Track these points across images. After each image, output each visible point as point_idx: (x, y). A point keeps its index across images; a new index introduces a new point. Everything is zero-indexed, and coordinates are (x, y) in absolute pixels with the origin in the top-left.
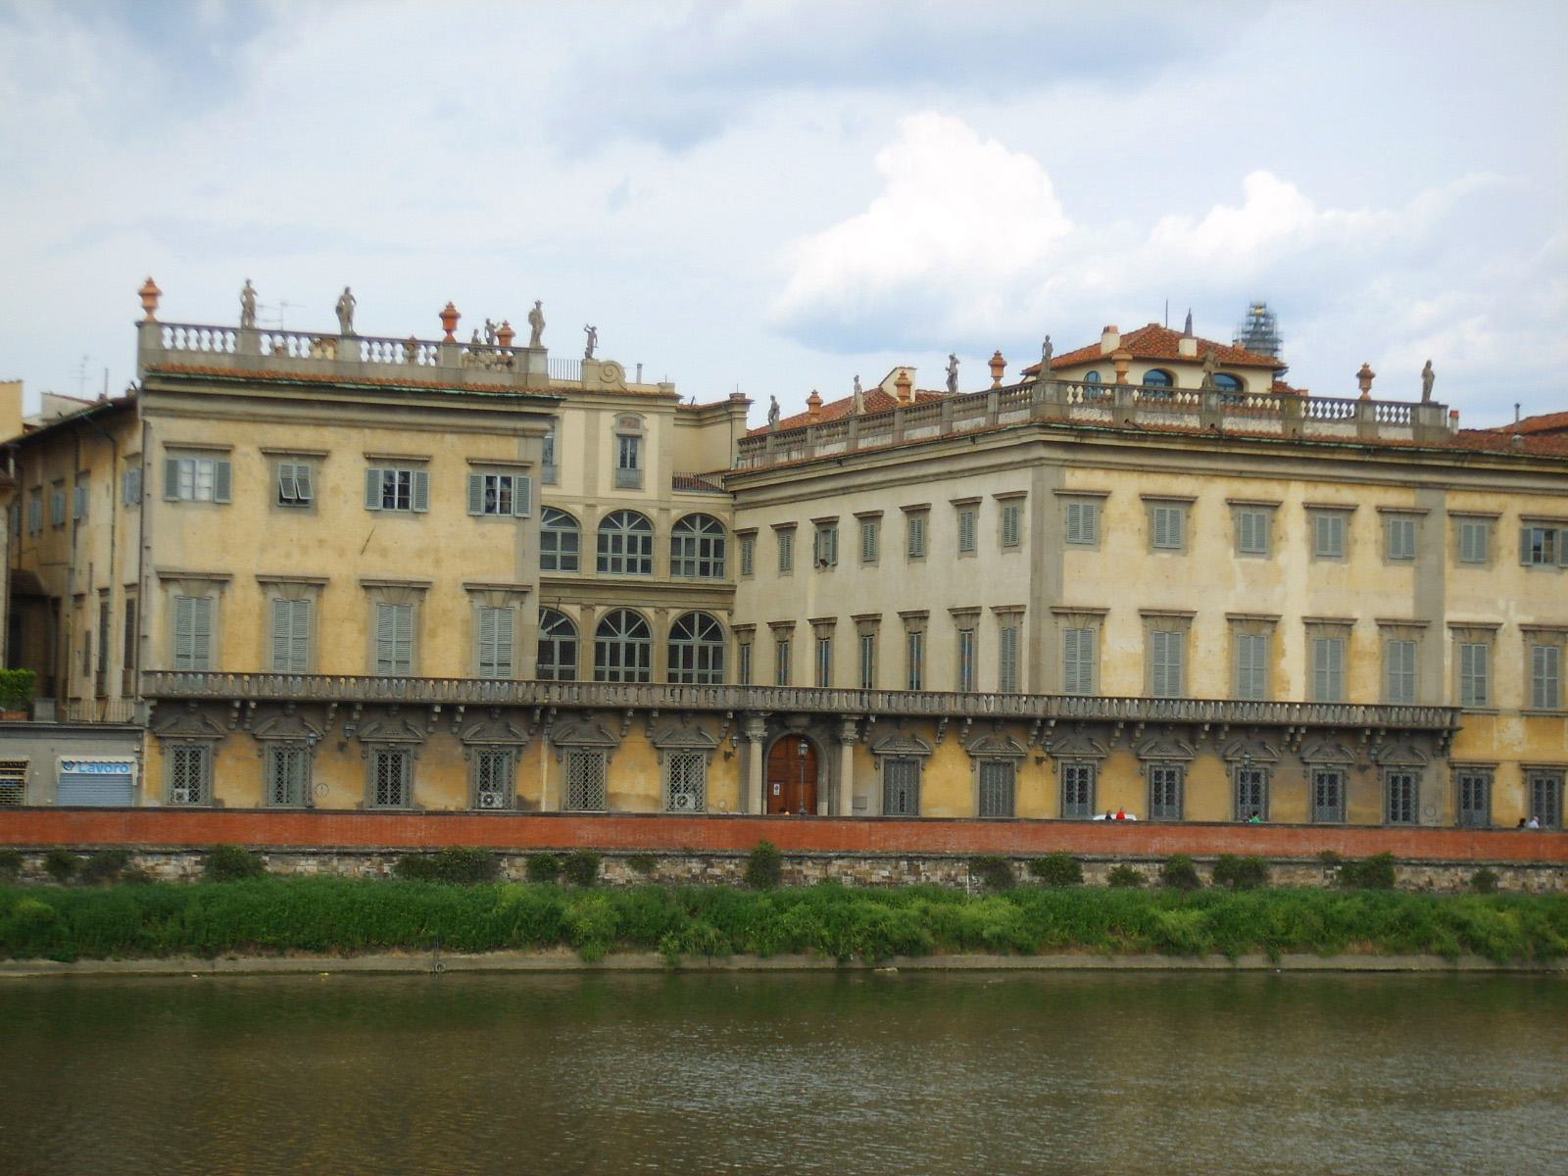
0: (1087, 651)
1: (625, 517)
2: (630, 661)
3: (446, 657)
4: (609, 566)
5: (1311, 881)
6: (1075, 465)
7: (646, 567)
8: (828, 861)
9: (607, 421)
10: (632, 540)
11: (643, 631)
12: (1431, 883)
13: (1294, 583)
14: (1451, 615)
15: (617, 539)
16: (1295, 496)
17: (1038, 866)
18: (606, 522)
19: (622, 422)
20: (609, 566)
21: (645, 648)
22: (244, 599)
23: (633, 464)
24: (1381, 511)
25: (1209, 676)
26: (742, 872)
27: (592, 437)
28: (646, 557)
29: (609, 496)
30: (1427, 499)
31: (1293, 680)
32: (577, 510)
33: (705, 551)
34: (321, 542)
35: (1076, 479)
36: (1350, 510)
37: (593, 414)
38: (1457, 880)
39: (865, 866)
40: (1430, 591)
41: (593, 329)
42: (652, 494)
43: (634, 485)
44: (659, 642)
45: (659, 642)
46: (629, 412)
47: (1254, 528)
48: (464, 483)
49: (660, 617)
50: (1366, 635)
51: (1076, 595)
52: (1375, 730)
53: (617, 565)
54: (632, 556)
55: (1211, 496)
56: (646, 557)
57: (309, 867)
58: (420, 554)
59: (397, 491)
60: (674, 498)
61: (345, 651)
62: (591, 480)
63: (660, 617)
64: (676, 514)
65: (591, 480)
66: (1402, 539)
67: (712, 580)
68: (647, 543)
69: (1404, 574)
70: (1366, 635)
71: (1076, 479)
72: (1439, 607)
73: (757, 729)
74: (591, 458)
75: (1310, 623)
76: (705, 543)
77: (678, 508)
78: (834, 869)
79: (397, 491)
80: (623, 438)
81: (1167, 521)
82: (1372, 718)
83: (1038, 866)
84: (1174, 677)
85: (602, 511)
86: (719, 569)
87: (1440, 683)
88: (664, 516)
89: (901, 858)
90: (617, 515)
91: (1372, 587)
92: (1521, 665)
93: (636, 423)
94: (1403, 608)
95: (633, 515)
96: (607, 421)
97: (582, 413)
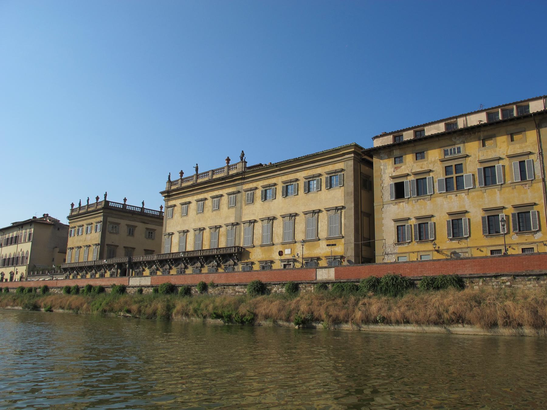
13: (210, 219)
30: (239, 188)
40: (239, 215)
69: (233, 210)
91: (226, 215)
94: (232, 220)
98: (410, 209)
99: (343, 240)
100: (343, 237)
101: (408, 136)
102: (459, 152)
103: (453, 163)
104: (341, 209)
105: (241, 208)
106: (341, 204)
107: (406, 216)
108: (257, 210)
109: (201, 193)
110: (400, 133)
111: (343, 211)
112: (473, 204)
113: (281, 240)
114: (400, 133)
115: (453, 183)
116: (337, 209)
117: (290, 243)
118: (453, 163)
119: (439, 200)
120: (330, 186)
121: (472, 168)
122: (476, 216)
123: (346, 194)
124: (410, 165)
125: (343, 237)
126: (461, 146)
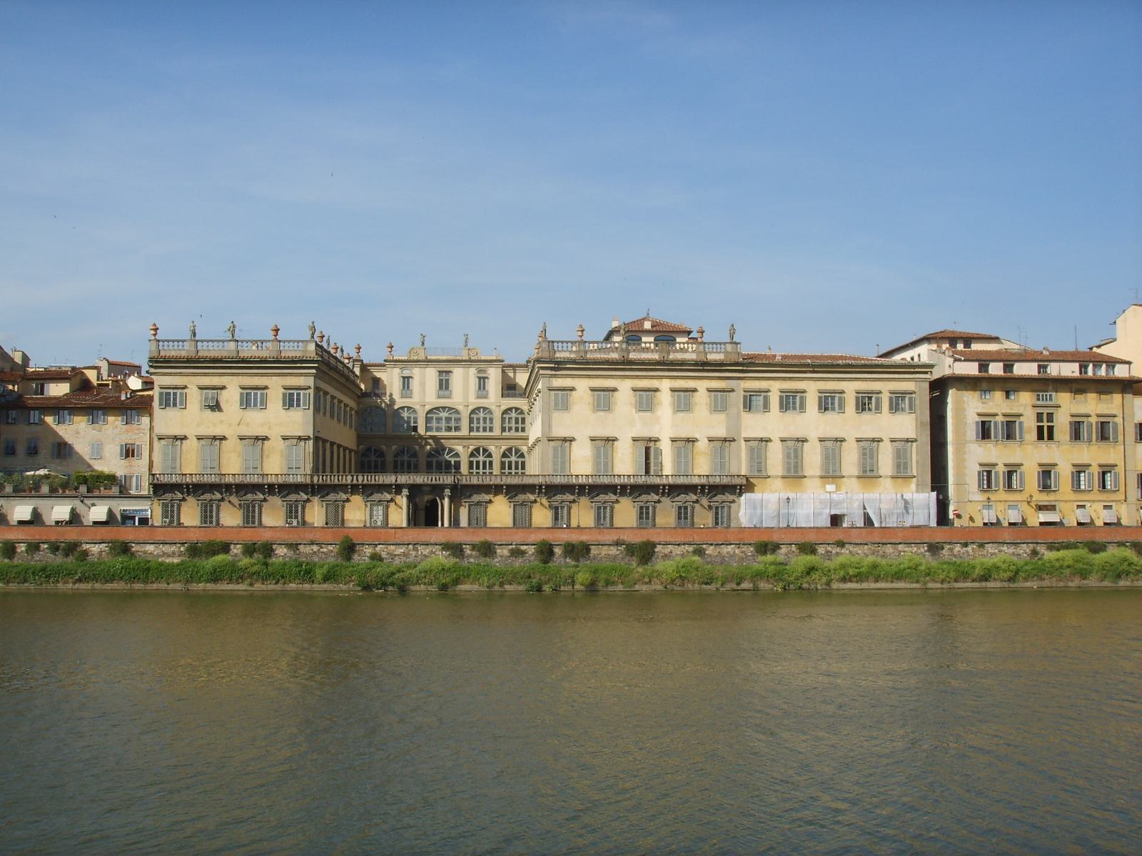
0: (563, 455)
2: (484, 468)
3: (275, 466)
4: (475, 430)
5: (610, 552)
6: (555, 376)
7: (491, 429)
8: (376, 545)
9: (472, 371)
11: (490, 455)
12: (671, 552)
13: (665, 423)
14: (745, 435)
16: (665, 385)
17: (474, 547)
18: (473, 412)
20: (475, 430)
21: (491, 463)
22: (191, 446)
23: (447, 388)
24: (673, 390)
25: (625, 465)
26: (335, 550)
27: (466, 378)
28: (523, 426)
29: (474, 402)
31: (668, 468)
32: (460, 408)
33: (517, 422)
34: (222, 422)
35: (558, 383)
36: (695, 390)
37: (466, 369)
38: (685, 551)
39: (392, 547)
40: (736, 424)
43: (486, 397)
44: (496, 460)
45: (496, 460)
47: (646, 399)
48: (281, 396)
49: (496, 450)
50: (702, 445)
51: (558, 432)
52: (703, 486)
53: (478, 430)
54: (517, 425)
55: (625, 387)
56: (523, 426)
57: (150, 548)
58: (262, 425)
59: (250, 398)
61: (233, 465)
62: (466, 395)
63: (496, 450)
64: (503, 408)
65: (466, 395)
66: (720, 400)
67: (520, 434)
68: (491, 420)
69: (721, 417)
70: (702, 445)
71: (558, 383)
72: (739, 430)
73: (405, 492)
74: (466, 386)
75: (673, 440)
78: (379, 548)
79: (250, 398)
80: (480, 378)
81: (603, 398)
82: (704, 481)
83: (474, 547)
84: (606, 465)
85: (471, 408)
86: (523, 430)
87: (740, 465)
89: (408, 544)
92: (780, 456)
93: (485, 371)
94: (721, 432)
95: (485, 409)
96: (472, 371)
98: (997, 453)
99: (914, 480)
100: (915, 477)
101: (996, 369)
102: (1051, 399)
103: (1045, 411)
104: (912, 442)
105: (739, 415)
106: (912, 435)
107: (993, 461)
108: (771, 424)
109: (645, 377)
110: (987, 363)
111: (914, 444)
112: (1063, 455)
113: (818, 473)
114: (987, 363)
115: (1045, 433)
116: (907, 441)
117: (834, 477)
118: (1045, 411)
119: (1029, 448)
120: (895, 407)
121: (1062, 422)
122: (1064, 472)
123: (920, 424)
124: (997, 404)
125: (915, 477)
126: (1054, 394)
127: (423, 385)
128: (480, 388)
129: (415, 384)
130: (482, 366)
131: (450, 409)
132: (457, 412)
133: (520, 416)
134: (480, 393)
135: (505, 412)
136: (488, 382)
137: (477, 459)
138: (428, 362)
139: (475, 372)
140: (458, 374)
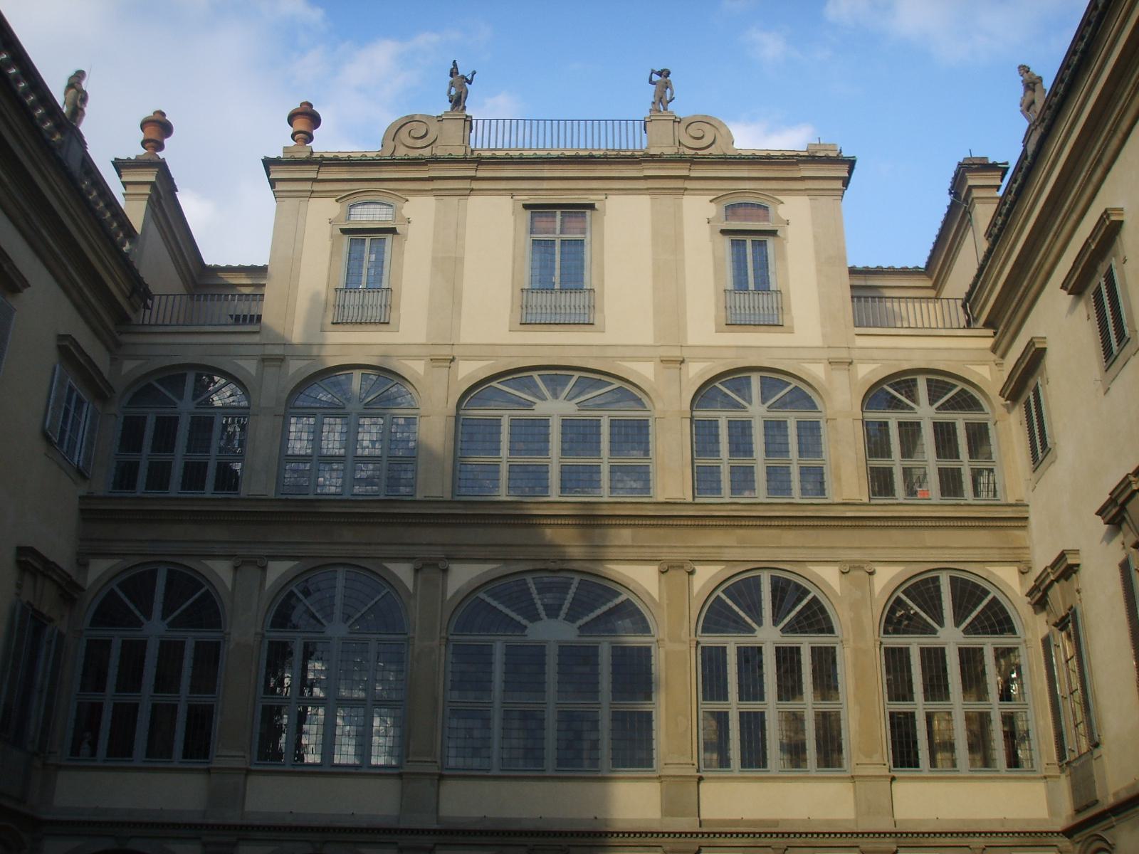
1: (755, 380)
2: (789, 688)
9: (699, 212)
10: (775, 429)
11: (815, 618)
15: (740, 432)
18: (705, 393)
19: (732, 210)
21: (825, 661)
27: (668, 242)
29: (711, 341)
32: (644, 372)
37: (667, 200)
41: (665, 73)
42: (809, 329)
44: (858, 645)
45: (858, 645)
46: (744, 192)
49: (855, 586)
60: (861, 342)
62: (670, 311)
63: (855, 586)
64: (867, 372)
65: (670, 311)
68: (810, 431)
76: (945, 434)
77: (874, 360)
85: (697, 372)
88: (840, 377)
90: (736, 377)
95: (773, 379)
96: (699, 212)
97: (645, 200)
127: (449, 267)
128: (740, 284)
129: (412, 267)
130: (748, 185)
131: (591, 377)
132: (628, 392)
133: (960, 420)
134: (741, 299)
135: (876, 396)
136: (782, 256)
137: (746, 640)
138: (482, 168)
139: (713, 210)
140: (625, 227)
